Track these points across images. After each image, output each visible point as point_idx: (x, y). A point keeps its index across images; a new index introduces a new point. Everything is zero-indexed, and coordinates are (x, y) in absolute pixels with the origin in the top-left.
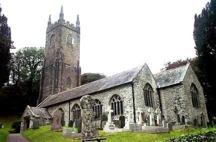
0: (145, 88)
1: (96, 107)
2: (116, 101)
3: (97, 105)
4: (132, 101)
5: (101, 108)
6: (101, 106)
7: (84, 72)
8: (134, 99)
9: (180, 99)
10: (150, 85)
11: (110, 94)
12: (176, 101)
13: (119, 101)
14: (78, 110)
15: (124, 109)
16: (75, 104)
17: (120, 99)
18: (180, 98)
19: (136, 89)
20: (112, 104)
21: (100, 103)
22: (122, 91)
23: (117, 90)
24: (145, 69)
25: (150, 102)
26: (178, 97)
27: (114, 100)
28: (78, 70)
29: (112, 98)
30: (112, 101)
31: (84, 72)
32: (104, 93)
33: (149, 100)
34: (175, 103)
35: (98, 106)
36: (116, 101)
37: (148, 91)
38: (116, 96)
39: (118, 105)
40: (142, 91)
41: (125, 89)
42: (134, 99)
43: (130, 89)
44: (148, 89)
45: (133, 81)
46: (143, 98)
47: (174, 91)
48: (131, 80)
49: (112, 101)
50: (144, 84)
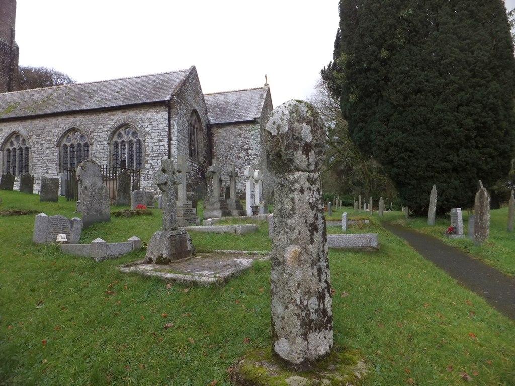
0: (189, 119)
2: (125, 138)
4: (166, 143)
6: (86, 145)
7: (25, 61)
8: (170, 139)
9: (250, 151)
10: (198, 116)
12: (243, 154)
13: (134, 140)
14: (20, 149)
16: (13, 133)
17: (134, 134)
18: (250, 149)
20: (116, 144)
23: (131, 113)
25: (194, 150)
26: (246, 146)
28: (12, 53)
29: (116, 131)
31: (25, 61)
33: (194, 146)
34: (239, 158)
35: (79, 145)
37: (194, 126)
39: (131, 149)
40: (186, 124)
41: (150, 114)
42: (170, 139)
43: (163, 114)
45: (171, 99)
46: (187, 140)
47: (240, 135)
48: (168, 97)
49: (115, 139)
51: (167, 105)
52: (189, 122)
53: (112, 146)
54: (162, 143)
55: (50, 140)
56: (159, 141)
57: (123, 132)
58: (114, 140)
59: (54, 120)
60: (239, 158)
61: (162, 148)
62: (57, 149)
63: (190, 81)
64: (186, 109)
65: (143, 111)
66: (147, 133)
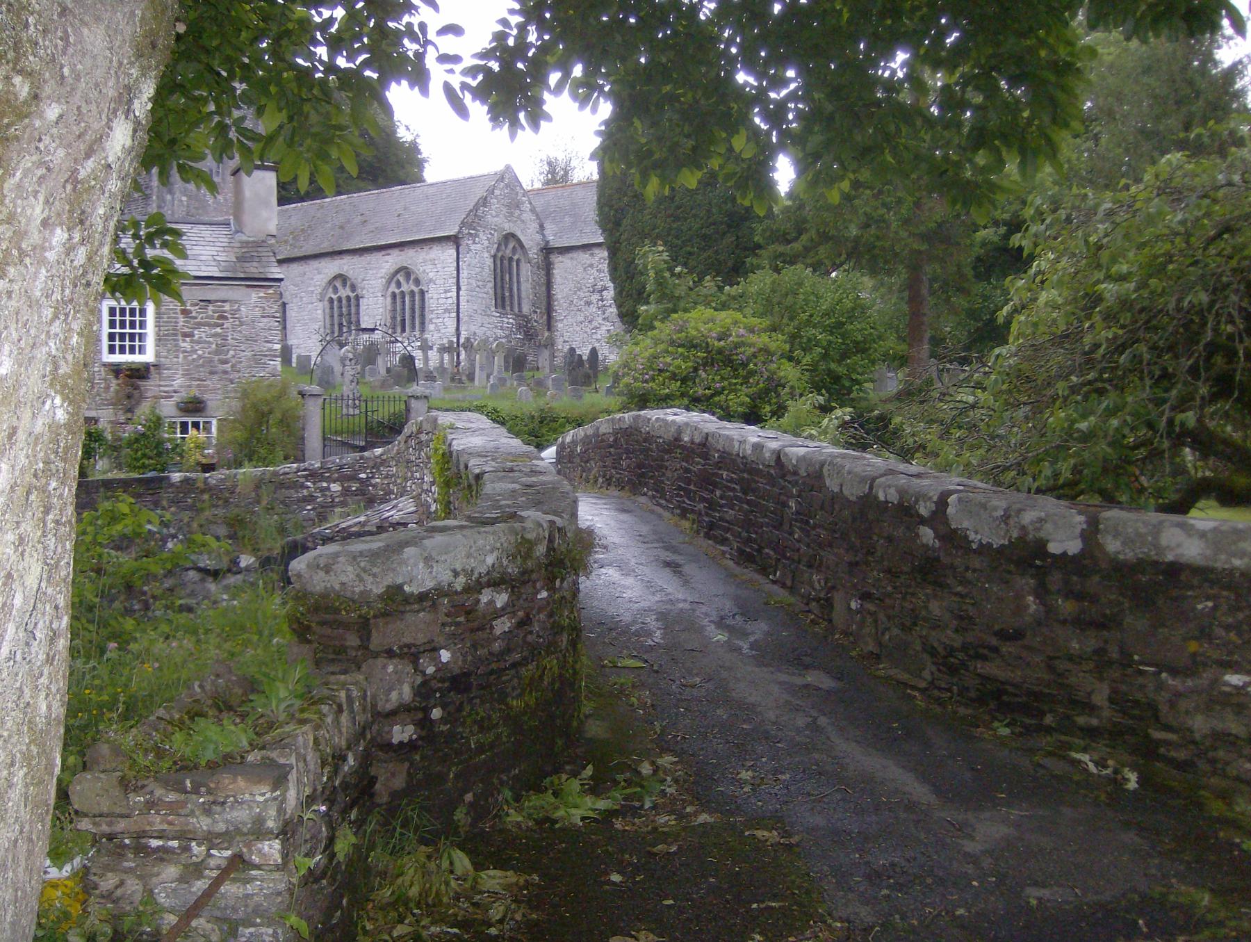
0: (498, 250)
1: (340, 300)
2: (405, 288)
3: (344, 292)
5: (358, 305)
6: (358, 298)
8: (459, 289)
10: (519, 241)
11: (389, 262)
15: (429, 316)
19: (466, 259)
20: (394, 296)
21: (353, 288)
22: (425, 261)
23: (410, 252)
24: (507, 186)
26: (599, 287)
27: (399, 284)
30: (393, 288)
32: (368, 258)
34: (589, 303)
35: (348, 298)
36: (405, 288)
37: (511, 259)
38: (406, 271)
39: (413, 302)
40: (489, 262)
42: (459, 289)
44: (508, 252)
47: (591, 266)
50: (496, 237)
51: (455, 240)
52: (500, 255)
53: (389, 300)
54: (449, 295)
55: (312, 292)
56: (446, 292)
57: (401, 279)
58: (391, 290)
59: (315, 264)
60: (589, 303)
61: (450, 301)
62: (321, 304)
63: (497, 192)
64: (488, 239)
65: (426, 248)
66: (431, 281)
